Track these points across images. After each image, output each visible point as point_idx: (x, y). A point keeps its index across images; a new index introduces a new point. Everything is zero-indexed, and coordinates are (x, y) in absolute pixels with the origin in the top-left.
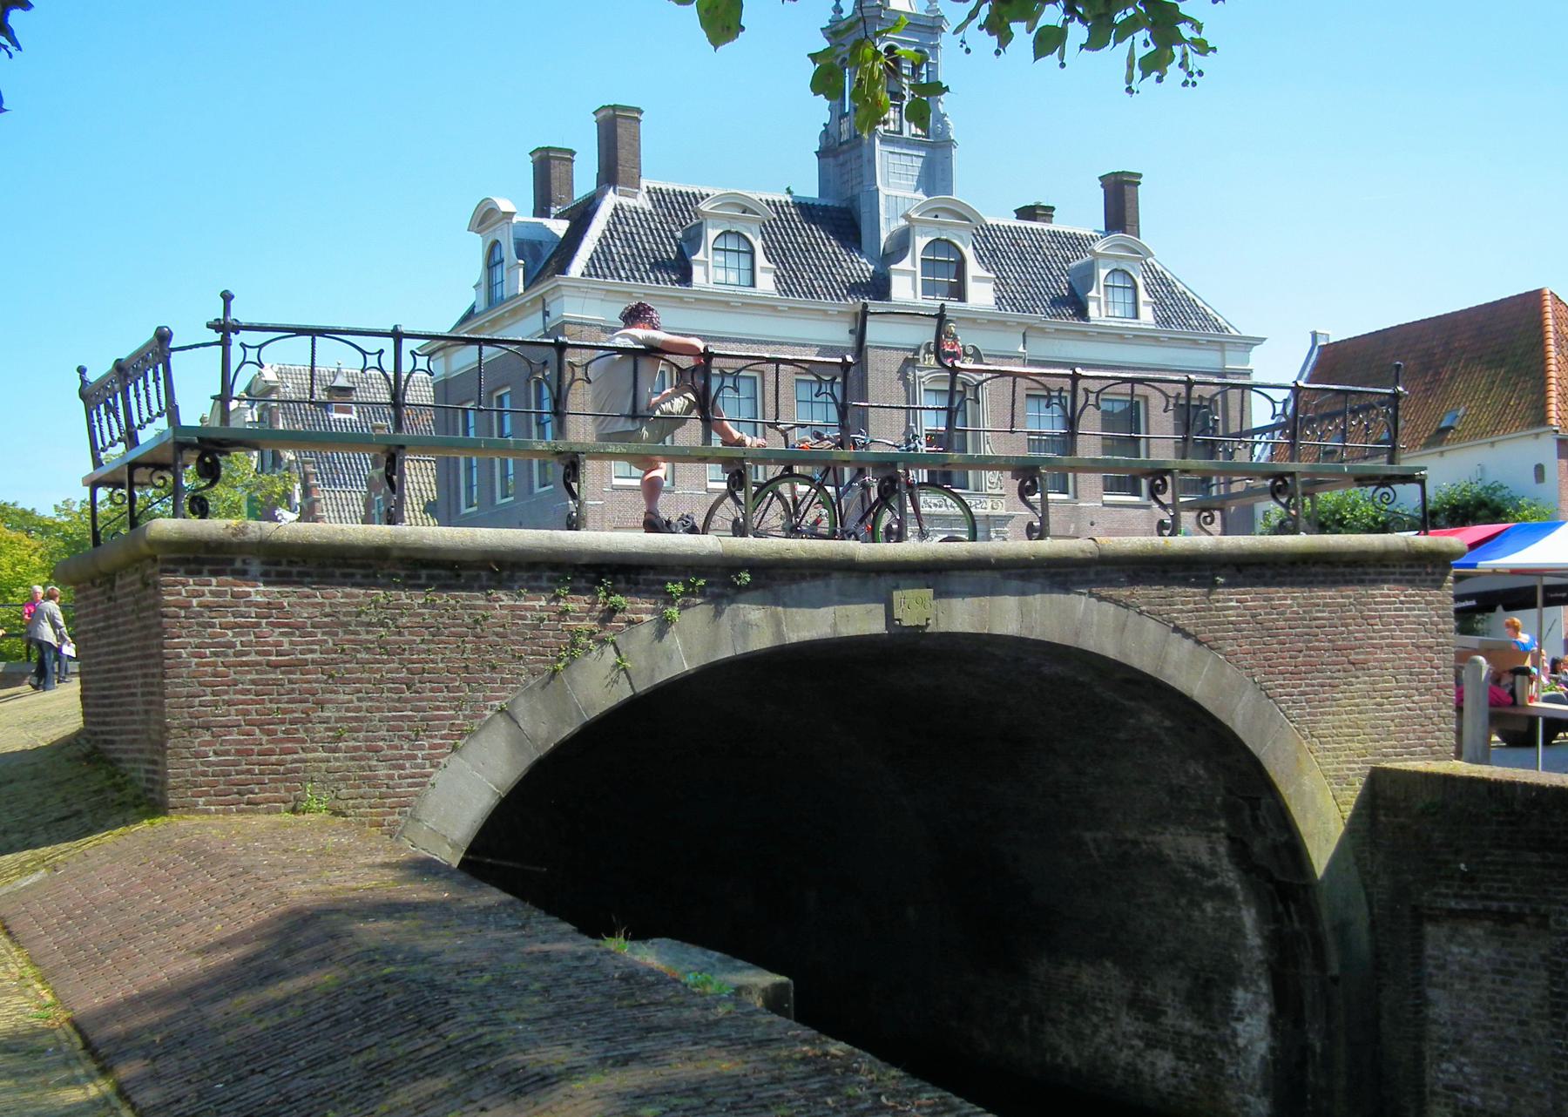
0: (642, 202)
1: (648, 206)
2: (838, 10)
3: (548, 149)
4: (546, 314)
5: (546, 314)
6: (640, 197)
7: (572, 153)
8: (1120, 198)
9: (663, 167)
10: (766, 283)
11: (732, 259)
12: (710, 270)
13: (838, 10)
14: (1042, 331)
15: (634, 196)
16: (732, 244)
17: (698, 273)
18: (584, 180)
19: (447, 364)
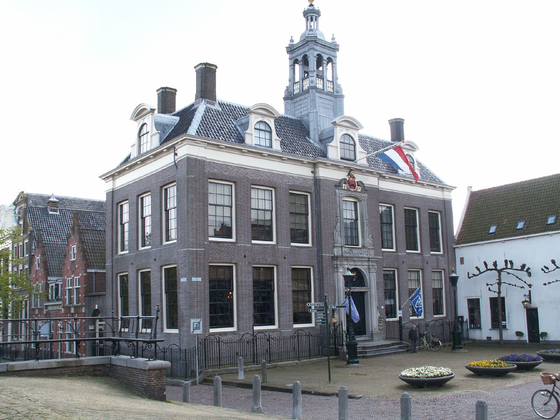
0: (217, 107)
1: (220, 109)
2: (292, 41)
3: (166, 88)
4: (176, 154)
5: (176, 154)
6: (216, 105)
7: (176, 90)
8: (397, 128)
9: (226, 92)
10: (277, 146)
11: (262, 134)
12: (252, 138)
13: (292, 41)
14: (384, 177)
15: (213, 104)
16: (262, 127)
17: (248, 140)
18: (182, 102)
19: (113, 184)
